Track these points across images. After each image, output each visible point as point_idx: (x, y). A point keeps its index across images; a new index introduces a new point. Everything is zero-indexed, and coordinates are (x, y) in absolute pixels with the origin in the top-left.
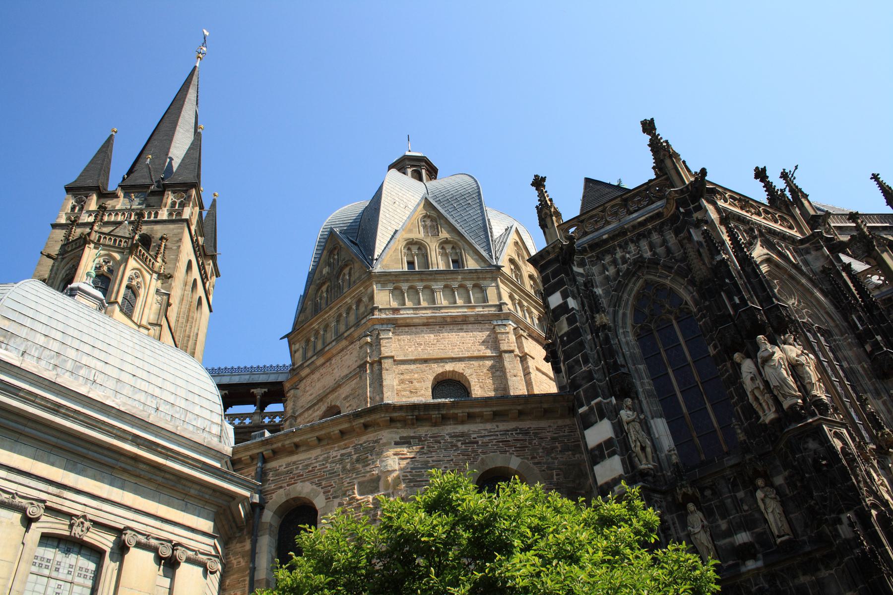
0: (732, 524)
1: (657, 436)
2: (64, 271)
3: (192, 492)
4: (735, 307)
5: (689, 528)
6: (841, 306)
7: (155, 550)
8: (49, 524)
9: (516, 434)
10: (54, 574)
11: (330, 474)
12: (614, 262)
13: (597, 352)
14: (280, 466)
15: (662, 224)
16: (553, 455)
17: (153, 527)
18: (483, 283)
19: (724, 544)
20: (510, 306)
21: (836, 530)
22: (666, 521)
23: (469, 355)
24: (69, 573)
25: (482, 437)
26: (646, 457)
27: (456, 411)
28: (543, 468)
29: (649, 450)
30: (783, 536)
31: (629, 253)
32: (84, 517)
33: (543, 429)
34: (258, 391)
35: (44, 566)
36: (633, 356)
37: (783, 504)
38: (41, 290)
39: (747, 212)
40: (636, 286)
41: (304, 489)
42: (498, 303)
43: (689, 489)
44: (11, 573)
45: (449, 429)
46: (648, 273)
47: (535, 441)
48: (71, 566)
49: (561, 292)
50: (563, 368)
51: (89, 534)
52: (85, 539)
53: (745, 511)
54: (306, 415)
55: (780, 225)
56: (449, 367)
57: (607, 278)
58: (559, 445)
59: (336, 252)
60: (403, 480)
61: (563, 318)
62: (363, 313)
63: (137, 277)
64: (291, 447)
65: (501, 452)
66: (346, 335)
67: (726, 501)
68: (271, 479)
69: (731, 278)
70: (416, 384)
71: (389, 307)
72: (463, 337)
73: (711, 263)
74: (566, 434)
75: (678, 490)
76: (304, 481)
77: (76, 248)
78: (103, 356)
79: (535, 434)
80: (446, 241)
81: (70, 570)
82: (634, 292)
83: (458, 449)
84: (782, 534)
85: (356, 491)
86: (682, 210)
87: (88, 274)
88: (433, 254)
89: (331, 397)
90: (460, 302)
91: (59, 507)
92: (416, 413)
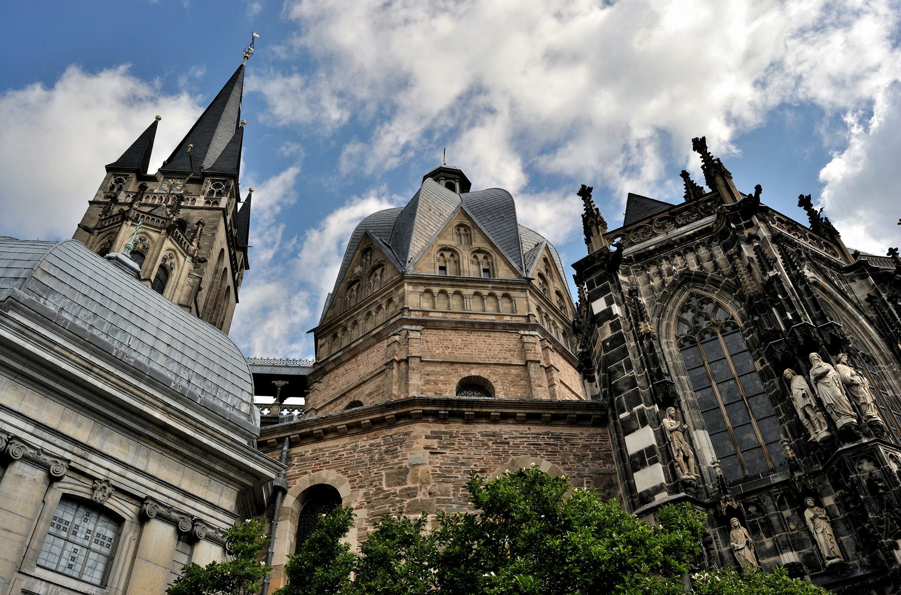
0: (777, 542)
1: (699, 448)
2: (99, 245)
3: (218, 468)
4: (787, 323)
5: (732, 544)
6: (886, 335)
7: (175, 523)
8: (71, 485)
9: (548, 438)
10: (72, 538)
11: (357, 463)
12: (660, 273)
13: (641, 360)
14: (306, 452)
15: (711, 240)
16: (584, 462)
17: (175, 500)
18: (513, 294)
19: (769, 563)
20: (537, 318)
21: (893, 555)
22: (708, 535)
23: (496, 362)
24: (86, 538)
25: (513, 438)
26: (688, 467)
27: (489, 410)
28: (573, 475)
29: (692, 460)
30: (833, 558)
31: (675, 265)
32: (107, 481)
33: (575, 435)
34: (280, 383)
35: (62, 528)
36: (675, 366)
37: (833, 525)
38: (82, 250)
39: (794, 235)
40: (681, 298)
41: (329, 476)
42: (527, 314)
43: (734, 503)
44: (30, 531)
45: (479, 429)
46: (693, 287)
47: (566, 447)
48: (89, 531)
49: (605, 298)
50: (597, 378)
51: (110, 500)
52: (106, 505)
53: (792, 530)
54: (327, 408)
55: (826, 251)
56: (474, 372)
57: (652, 289)
58: (590, 453)
59: (369, 253)
60: (432, 474)
61: (607, 324)
62: (393, 313)
63: (171, 258)
64: (320, 433)
65: (532, 455)
66: (374, 333)
67: (772, 518)
68: (296, 464)
69: (785, 294)
70: (443, 387)
71: (419, 309)
72: (490, 344)
73: (762, 279)
74: (598, 442)
75: (722, 504)
76: (330, 468)
77: (113, 224)
78: (139, 323)
79: (567, 440)
80: (479, 251)
81: (88, 535)
82: (679, 304)
83: (489, 448)
85: (384, 483)
86: (733, 226)
87: (127, 247)
88: (466, 262)
89: (355, 392)
90: (490, 308)
91: (83, 469)
92: (450, 409)
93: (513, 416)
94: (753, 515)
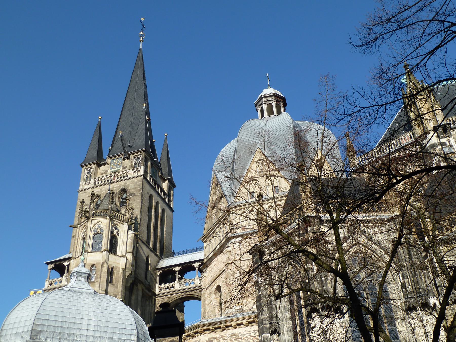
25: (244, 335)
34: (196, 265)
89: (218, 280)
92: (214, 326)
93: (242, 324)
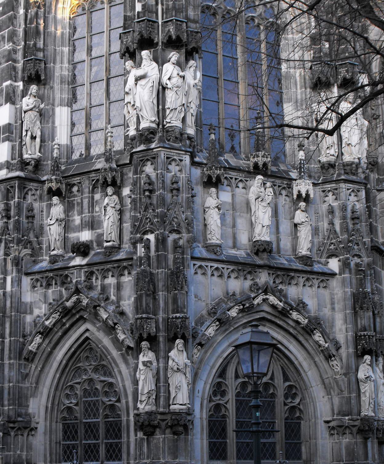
19: (73, 237)
30: (109, 241)
53: (96, 212)
84: (109, 239)
94: (75, 195)
